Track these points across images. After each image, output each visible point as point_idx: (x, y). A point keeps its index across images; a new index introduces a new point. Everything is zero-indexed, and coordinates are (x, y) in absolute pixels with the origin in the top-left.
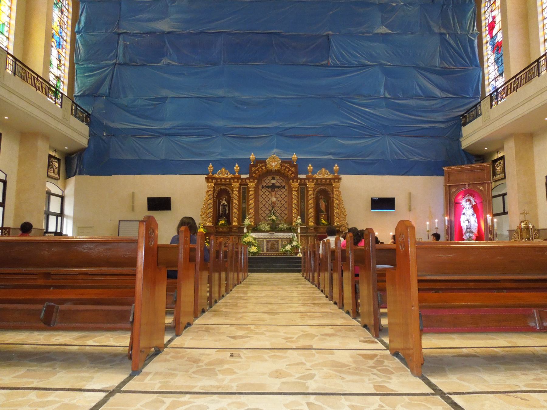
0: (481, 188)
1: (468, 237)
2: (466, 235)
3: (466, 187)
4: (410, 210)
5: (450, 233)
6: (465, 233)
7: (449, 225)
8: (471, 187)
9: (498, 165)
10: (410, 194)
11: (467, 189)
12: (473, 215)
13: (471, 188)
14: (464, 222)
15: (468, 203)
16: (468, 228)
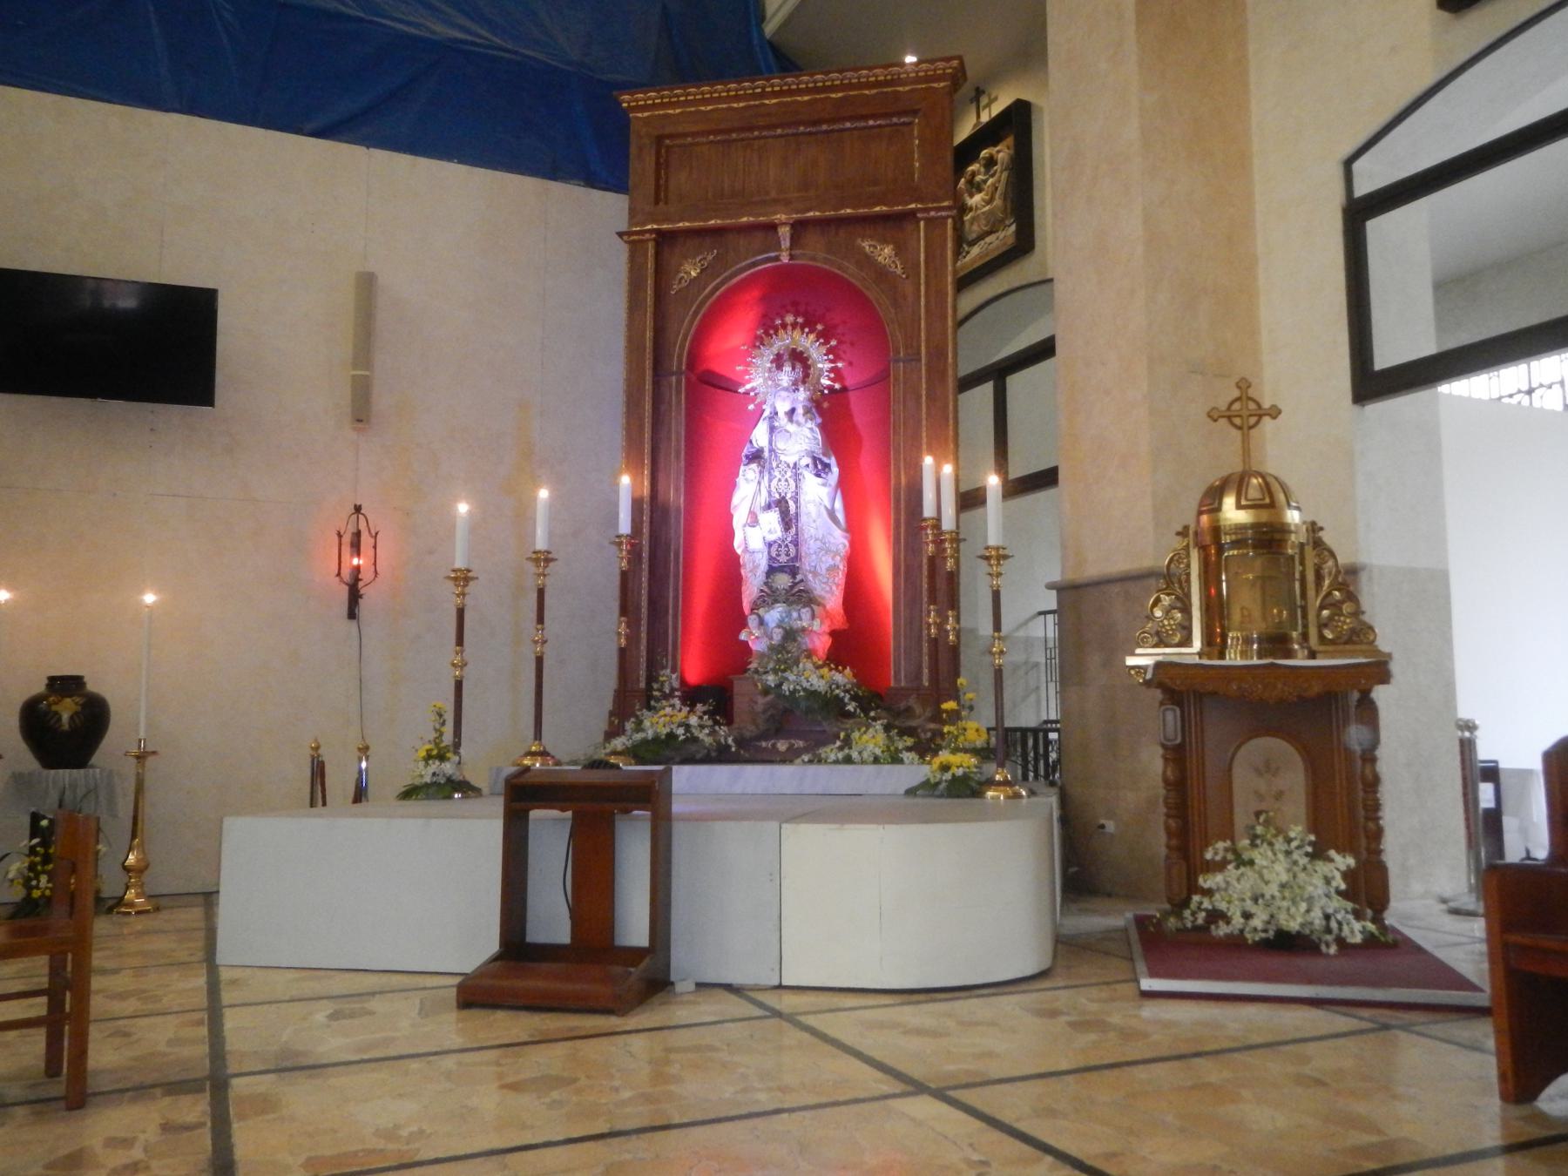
0: (885, 254)
1: (777, 636)
2: (762, 622)
3: (778, 247)
4: (361, 414)
5: (652, 602)
6: (755, 607)
7: (645, 542)
8: (814, 240)
9: (979, 178)
10: (367, 284)
11: (785, 259)
12: (821, 469)
13: (816, 254)
14: (753, 521)
15: (786, 377)
16: (782, 569)
